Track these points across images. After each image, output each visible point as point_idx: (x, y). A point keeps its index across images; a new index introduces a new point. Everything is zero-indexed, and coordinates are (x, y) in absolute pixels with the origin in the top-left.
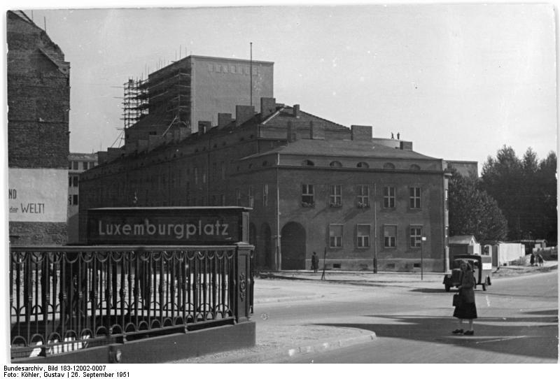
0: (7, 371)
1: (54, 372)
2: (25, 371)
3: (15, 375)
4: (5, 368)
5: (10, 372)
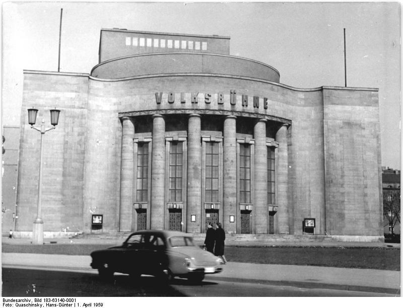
0: (5, 302)
1: (39, 303)
2: (18, 302)
3: (11, 305)
4: (4, 300)
5: (7, 303)
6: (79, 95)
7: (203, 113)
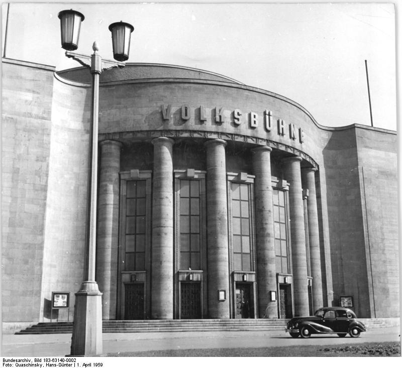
0: (5, 362)
1: (39, 363)
4: (4, 360)
5: (7, 363)
6: (38, 98)
7: (230, 139)
